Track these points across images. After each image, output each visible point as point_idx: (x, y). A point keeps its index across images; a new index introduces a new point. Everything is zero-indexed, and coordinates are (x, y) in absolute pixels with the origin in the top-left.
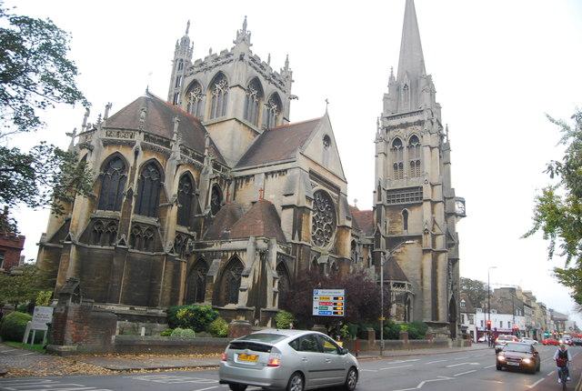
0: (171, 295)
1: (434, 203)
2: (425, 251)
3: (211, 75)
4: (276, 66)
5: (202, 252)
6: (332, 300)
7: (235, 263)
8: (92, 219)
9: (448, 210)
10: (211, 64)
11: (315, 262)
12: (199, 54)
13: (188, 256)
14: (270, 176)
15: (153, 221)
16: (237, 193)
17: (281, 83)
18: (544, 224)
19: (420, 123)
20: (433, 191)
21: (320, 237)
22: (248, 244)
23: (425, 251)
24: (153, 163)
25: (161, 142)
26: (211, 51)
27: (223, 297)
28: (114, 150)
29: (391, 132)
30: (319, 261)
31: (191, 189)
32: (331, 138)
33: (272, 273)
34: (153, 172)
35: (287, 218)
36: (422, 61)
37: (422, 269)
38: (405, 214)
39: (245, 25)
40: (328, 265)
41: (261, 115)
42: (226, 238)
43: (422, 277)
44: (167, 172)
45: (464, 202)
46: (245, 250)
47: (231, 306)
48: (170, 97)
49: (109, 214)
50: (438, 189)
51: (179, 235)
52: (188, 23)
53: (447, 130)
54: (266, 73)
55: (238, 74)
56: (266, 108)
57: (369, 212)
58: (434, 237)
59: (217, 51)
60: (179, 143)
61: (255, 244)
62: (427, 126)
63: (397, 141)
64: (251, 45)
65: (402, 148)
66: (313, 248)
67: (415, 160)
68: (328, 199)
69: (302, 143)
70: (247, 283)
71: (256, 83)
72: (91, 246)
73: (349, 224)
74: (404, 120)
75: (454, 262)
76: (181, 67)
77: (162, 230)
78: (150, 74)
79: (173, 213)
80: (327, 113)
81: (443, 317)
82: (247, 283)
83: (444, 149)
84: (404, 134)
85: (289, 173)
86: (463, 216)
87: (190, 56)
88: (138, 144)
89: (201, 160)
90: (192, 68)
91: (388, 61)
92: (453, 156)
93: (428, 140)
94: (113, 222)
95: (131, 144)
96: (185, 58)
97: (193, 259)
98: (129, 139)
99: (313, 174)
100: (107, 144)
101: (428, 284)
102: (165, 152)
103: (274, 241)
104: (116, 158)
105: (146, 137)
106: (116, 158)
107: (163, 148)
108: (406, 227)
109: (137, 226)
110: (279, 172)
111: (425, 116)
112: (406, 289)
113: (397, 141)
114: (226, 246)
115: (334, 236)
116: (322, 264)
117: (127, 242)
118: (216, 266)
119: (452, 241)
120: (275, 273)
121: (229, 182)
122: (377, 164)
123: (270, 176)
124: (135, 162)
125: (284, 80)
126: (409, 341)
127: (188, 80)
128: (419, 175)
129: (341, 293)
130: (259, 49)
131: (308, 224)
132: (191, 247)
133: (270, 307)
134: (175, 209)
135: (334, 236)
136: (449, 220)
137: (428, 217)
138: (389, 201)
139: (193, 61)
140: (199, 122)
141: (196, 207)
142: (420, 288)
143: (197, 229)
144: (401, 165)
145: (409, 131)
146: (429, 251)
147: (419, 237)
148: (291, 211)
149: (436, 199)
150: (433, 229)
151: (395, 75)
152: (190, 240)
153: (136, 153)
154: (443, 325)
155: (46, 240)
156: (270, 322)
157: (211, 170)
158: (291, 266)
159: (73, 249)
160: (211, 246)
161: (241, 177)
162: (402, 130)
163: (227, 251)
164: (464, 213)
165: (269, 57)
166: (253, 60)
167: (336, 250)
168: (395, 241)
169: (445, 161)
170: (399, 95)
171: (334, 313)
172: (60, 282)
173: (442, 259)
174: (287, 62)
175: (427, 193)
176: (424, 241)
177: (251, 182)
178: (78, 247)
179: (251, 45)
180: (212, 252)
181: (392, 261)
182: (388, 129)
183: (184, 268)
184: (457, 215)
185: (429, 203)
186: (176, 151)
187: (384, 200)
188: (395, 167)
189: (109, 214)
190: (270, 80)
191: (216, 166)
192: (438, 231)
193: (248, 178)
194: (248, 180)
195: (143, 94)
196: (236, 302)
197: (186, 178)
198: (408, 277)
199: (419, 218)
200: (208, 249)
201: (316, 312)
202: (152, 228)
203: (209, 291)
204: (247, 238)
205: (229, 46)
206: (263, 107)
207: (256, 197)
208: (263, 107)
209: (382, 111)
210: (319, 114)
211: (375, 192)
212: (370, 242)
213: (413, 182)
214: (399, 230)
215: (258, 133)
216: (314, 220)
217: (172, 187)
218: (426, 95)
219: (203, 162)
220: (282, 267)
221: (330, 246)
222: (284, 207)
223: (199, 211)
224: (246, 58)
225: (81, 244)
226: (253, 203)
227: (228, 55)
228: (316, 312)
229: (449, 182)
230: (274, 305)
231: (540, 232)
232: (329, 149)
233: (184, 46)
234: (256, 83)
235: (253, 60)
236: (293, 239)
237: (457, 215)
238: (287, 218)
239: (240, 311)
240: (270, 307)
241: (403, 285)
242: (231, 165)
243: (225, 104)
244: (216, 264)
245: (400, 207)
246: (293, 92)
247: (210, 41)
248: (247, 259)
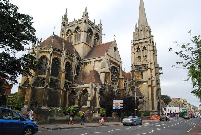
0: (64, 103)
1: (151, 70)
2: (149, 86)
3: (75, 27)
4: (97, 24)
6: (119, 104)
7: (85, 91)
8: (36, 78)
9: (156, 72)
11: (112, 91)
12: (70, 20)
13: (69, 90)
14: (96, 62)
15: (57, 78)
16: (85, 68)
17: (99, 30)
18: (191, 77)
19: (146, 42)
20: (151, 65)
21: (114, 82)
22: (90, 85)
23: (149, 86)
24: (56, 58)
25: (59, 51)
26: (74, 19)
27: (81, 103)
28: (43, 54)
29: (137, 46)
30: (114, 91)
31: (70, 67)
32: (117, 49)
33: (98, 96)
34: (56, 62)
35: (102, 76)
36: (147, 21)
37: (148, 92)
38: (142, 73)
39: (86, 10)
40: (117, 92)
41: (92, 41)
42: (82, 83)
43: (148, 94)
44: (61, 61)
45: (162, 69)
46: (89, 87)
47: (84, 107)
48: (61, 35)
49: (42, 76)
50: (153, 65)
51: (66, 83)
52: (66, 10)
53: (155, 44)
54: (94, 26)
55: (83, 27)
56: (94, 38)
57: (129, 73)
58: (152, 81)
59: (77, 19)
60: (65, 51)
61: (92, 85)
62: (149, 43)
63: (138, 48)
64: (88, 17)
65: (140, 51)
66: (112, 86)
67: (145, 55)
68: (115, 68)
69: (107, 50)
70: (89, 98)
71: (90, 30)
72: (36, 87)
73: (123, 77)
74: (141, 41)
75: (159, 89)
76: (64, 25)
77: (60, 81)
78: (54, 28)
79: (63, 76)
80: (115, 40)
81: (156, 109)
82: (89, 98)
83: (154, 51)
84: (141, 46)
85: (103, 61)
86: (162, 74)
87: (67, 21)
88: (51, 52)
89: (73, 57)
90: (68, 25)
91: (135, 21)
92: (158, 53)
93: (149, 48)
94: (43, 79)
95: (49, 52)
96: (65, 22)
97: (71, 91)
98: (48, 50)
99: (111, 61)
100: (40, 52)
101: (150, 97)
103: (98, 84)
104: (44, 57)
105: (54, 50)
106: (44, 57)
107: (60, 53)
108: (142, 78)
109: (51, 80)
110: (99, 60)
111: (148, 40)
112: (143, 99)
113: (138, 48)
114: (82, 86)
115: (118, 81)
116: (115, 92)
117: (48, 86)
118: (79, 93)
119: (158, 82)
120: (99, 95)
121: (82, 64)
122: (132, 57)
123: (96, 62)
124: (51, 58)
125: (99, 29)
126: (145, 117)
127: (67, 30)
128: (146, 60)
129: (122, 101)
130: (91, 18)
131: (109, 78)
132: (70, 87)
133: (98, 106)
134: (64, 74)
135: (118, 81)
136: (157, 75)
137: (150, 74)
138: (136, 69)
139: (68, 23)
140: (71, 44)
142: (148, 99)
143: (72, 80)
144: (140, 57)
145: (142, 45)
146: (151, 86)
147: (147, 81)
148: (104, 73)
149: (152, 68)
150: (152, 79)
151: (137, 26)
153: (51, 55)
154: (156, 111)
155: (21, 85)
156: (98, 112)
157: (76, 60)
158: (105, 93)
159: (30, 88)
160: (77, 86)
161: (86, 62)
162: (140, 45)
163: (82, 88)
164: (162, 72)
165: (94, 21)
166: (89, 22)
167: (119, 87)
168: (139, 83)
169: (155, 55)
170: (139, 34)
171: (120, 108)
172: (26, 100)
173: (155, 89)
174: (100, 22)
175: (149, 66)
176: (149, 83)
177: (90, 64)
178: (32, 88)
179: (88, 17)
180: (77, 88)
181: (138, 90)
182: (135, 44)
183: (68, 94)
184: (159, 74)
185: (150, 69)
186: (64, 54)
187: (135, 69)
188: (138, 57)
189: (42, 76)
190: (95, 29)
191: (78, 59)
192: (153, 79)
193: (88, 62)
194: (88, 64)
195: (52, 35)
196: (86, 105)
197: (68, 63)
198: (144, 95)
199: (147, 75)
200: (76, 87)
201: (114, 108)
202: (57, 81)
203: (77, 102)
204: (89, 83)
205: (81, 17)
206: (93, 38)
207: (92, 69)
208: (93, 38)
209: (133, 38)
210: (113, 40)
211: (131, 66)
212: (130, 83)
213: (144, 62)
214: (140, 79)
215: (91, 47)
216: (111, 77)
217: (63, 66)
218: (148, 33)
219: (73, 58)
220: (101, 93)
221: (117, 85)
222: (101, 72)
223: (72, 74)
224: (87, 22)
225: (33, 87)
226: (91, 71)
227: (80, 21)
228: (114, 108)
229: (157, 62)
230: (99, 106)
231: (190, 80)
232: (116, 52)
233: (65, 18)
234: (90, 30)
235: (89, 22)
236: (105, 83)
237: (159, 74)
238: (102, 76)
239: (87, 108)
240: (98, 106)
241: (142, 98)
242: (82, 58)
243: (80, 38)
245: (140, 71)
246: (103, 33)
247: (75, 16)
248: (89, 91)
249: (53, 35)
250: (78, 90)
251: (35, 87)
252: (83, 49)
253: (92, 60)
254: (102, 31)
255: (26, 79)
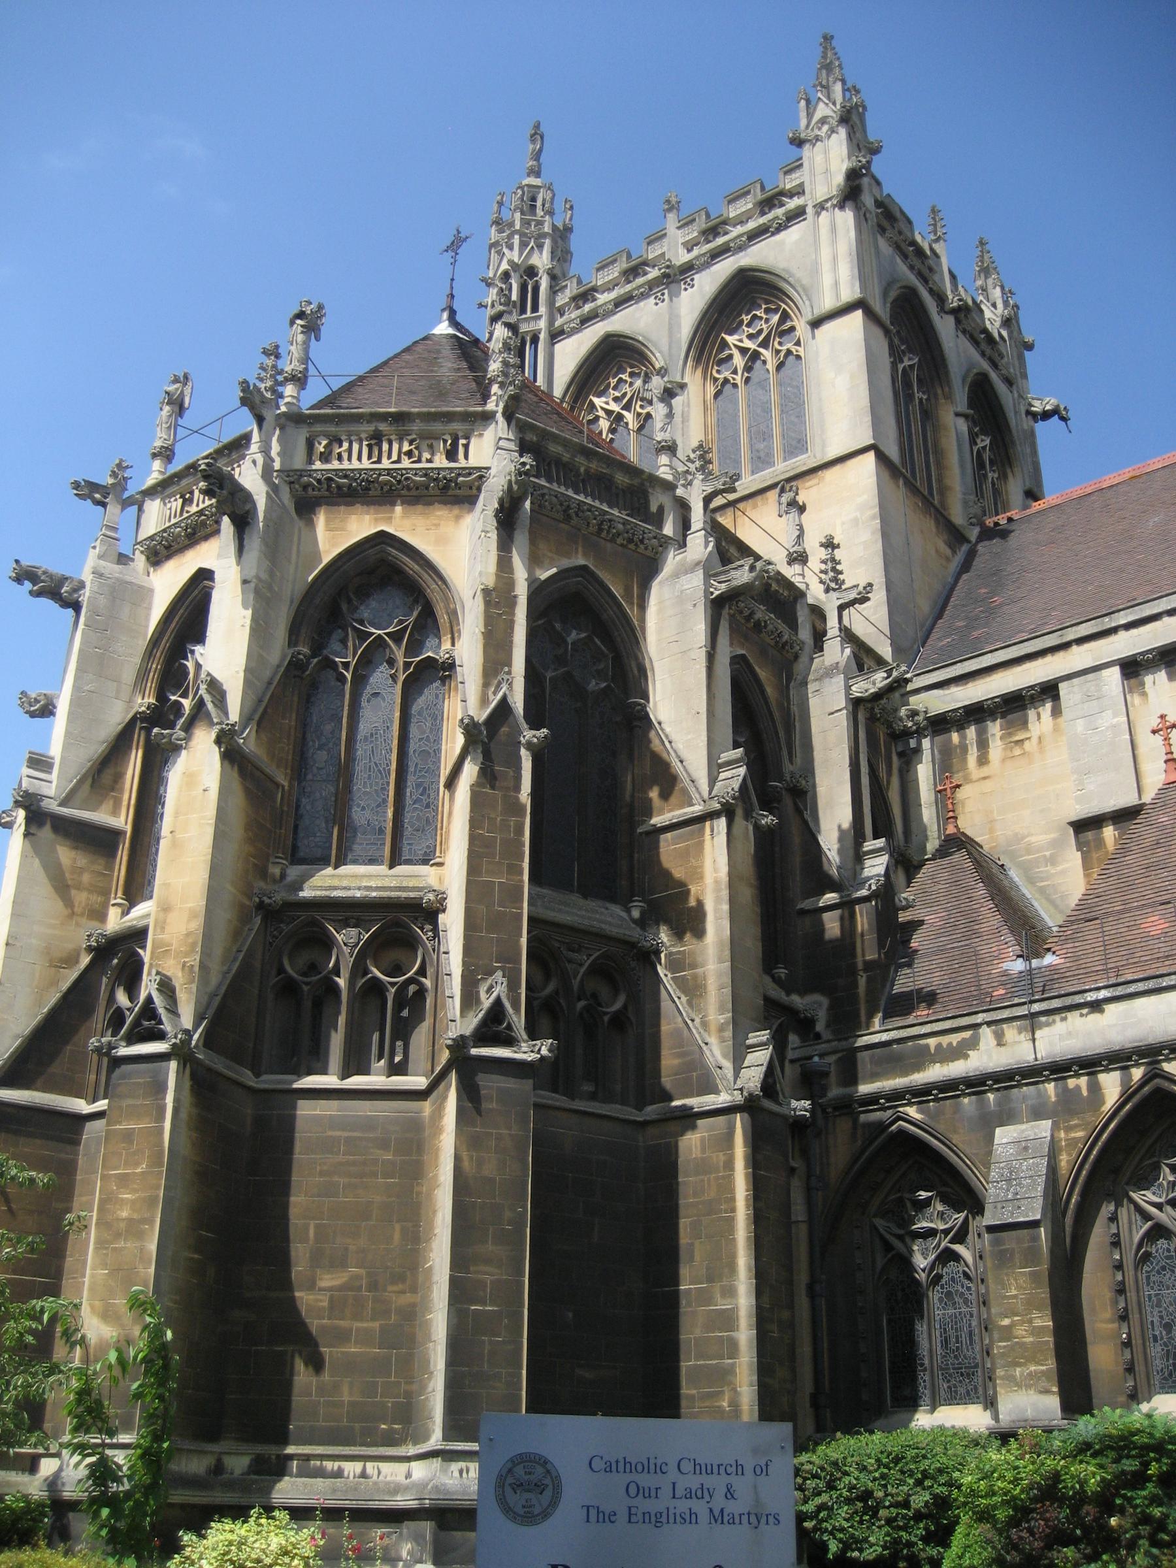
5: (897, 1096)
10: (682, 257)
52: (537, 134)
87: (562, 255)
90: (585, 296)
96: (542, 260)
98: (440, 461)
102: (633, 540)
117: (518, 1020)
139: (582, 267)
141: (797, 860)
152: (793, 1039)
160: (958, 1052)
161: (977, 713)
163: (1090, 1064)
200: (935, 1073)
225: (220, 1064)
244: (1023, 1147)
249: (451, 331)
250: (1006, 1117)
251: (247, 1077)
252: (885, 535)
253: (1079, 658)
254: (1025, 376)
255: (70, 960)
